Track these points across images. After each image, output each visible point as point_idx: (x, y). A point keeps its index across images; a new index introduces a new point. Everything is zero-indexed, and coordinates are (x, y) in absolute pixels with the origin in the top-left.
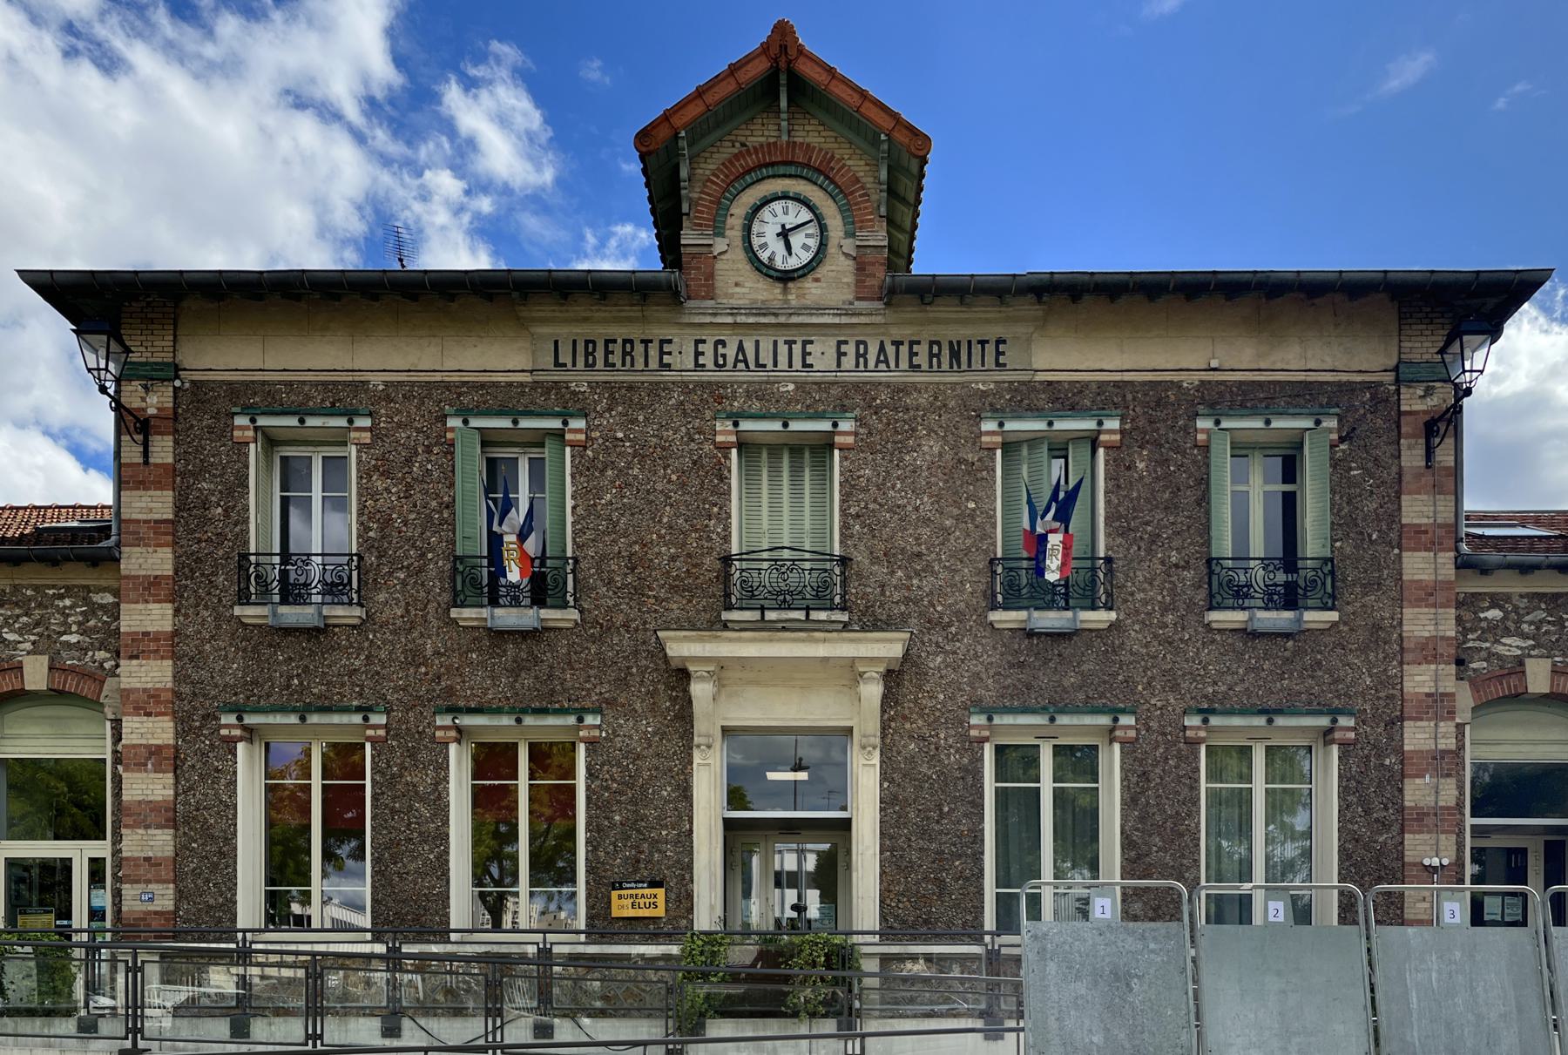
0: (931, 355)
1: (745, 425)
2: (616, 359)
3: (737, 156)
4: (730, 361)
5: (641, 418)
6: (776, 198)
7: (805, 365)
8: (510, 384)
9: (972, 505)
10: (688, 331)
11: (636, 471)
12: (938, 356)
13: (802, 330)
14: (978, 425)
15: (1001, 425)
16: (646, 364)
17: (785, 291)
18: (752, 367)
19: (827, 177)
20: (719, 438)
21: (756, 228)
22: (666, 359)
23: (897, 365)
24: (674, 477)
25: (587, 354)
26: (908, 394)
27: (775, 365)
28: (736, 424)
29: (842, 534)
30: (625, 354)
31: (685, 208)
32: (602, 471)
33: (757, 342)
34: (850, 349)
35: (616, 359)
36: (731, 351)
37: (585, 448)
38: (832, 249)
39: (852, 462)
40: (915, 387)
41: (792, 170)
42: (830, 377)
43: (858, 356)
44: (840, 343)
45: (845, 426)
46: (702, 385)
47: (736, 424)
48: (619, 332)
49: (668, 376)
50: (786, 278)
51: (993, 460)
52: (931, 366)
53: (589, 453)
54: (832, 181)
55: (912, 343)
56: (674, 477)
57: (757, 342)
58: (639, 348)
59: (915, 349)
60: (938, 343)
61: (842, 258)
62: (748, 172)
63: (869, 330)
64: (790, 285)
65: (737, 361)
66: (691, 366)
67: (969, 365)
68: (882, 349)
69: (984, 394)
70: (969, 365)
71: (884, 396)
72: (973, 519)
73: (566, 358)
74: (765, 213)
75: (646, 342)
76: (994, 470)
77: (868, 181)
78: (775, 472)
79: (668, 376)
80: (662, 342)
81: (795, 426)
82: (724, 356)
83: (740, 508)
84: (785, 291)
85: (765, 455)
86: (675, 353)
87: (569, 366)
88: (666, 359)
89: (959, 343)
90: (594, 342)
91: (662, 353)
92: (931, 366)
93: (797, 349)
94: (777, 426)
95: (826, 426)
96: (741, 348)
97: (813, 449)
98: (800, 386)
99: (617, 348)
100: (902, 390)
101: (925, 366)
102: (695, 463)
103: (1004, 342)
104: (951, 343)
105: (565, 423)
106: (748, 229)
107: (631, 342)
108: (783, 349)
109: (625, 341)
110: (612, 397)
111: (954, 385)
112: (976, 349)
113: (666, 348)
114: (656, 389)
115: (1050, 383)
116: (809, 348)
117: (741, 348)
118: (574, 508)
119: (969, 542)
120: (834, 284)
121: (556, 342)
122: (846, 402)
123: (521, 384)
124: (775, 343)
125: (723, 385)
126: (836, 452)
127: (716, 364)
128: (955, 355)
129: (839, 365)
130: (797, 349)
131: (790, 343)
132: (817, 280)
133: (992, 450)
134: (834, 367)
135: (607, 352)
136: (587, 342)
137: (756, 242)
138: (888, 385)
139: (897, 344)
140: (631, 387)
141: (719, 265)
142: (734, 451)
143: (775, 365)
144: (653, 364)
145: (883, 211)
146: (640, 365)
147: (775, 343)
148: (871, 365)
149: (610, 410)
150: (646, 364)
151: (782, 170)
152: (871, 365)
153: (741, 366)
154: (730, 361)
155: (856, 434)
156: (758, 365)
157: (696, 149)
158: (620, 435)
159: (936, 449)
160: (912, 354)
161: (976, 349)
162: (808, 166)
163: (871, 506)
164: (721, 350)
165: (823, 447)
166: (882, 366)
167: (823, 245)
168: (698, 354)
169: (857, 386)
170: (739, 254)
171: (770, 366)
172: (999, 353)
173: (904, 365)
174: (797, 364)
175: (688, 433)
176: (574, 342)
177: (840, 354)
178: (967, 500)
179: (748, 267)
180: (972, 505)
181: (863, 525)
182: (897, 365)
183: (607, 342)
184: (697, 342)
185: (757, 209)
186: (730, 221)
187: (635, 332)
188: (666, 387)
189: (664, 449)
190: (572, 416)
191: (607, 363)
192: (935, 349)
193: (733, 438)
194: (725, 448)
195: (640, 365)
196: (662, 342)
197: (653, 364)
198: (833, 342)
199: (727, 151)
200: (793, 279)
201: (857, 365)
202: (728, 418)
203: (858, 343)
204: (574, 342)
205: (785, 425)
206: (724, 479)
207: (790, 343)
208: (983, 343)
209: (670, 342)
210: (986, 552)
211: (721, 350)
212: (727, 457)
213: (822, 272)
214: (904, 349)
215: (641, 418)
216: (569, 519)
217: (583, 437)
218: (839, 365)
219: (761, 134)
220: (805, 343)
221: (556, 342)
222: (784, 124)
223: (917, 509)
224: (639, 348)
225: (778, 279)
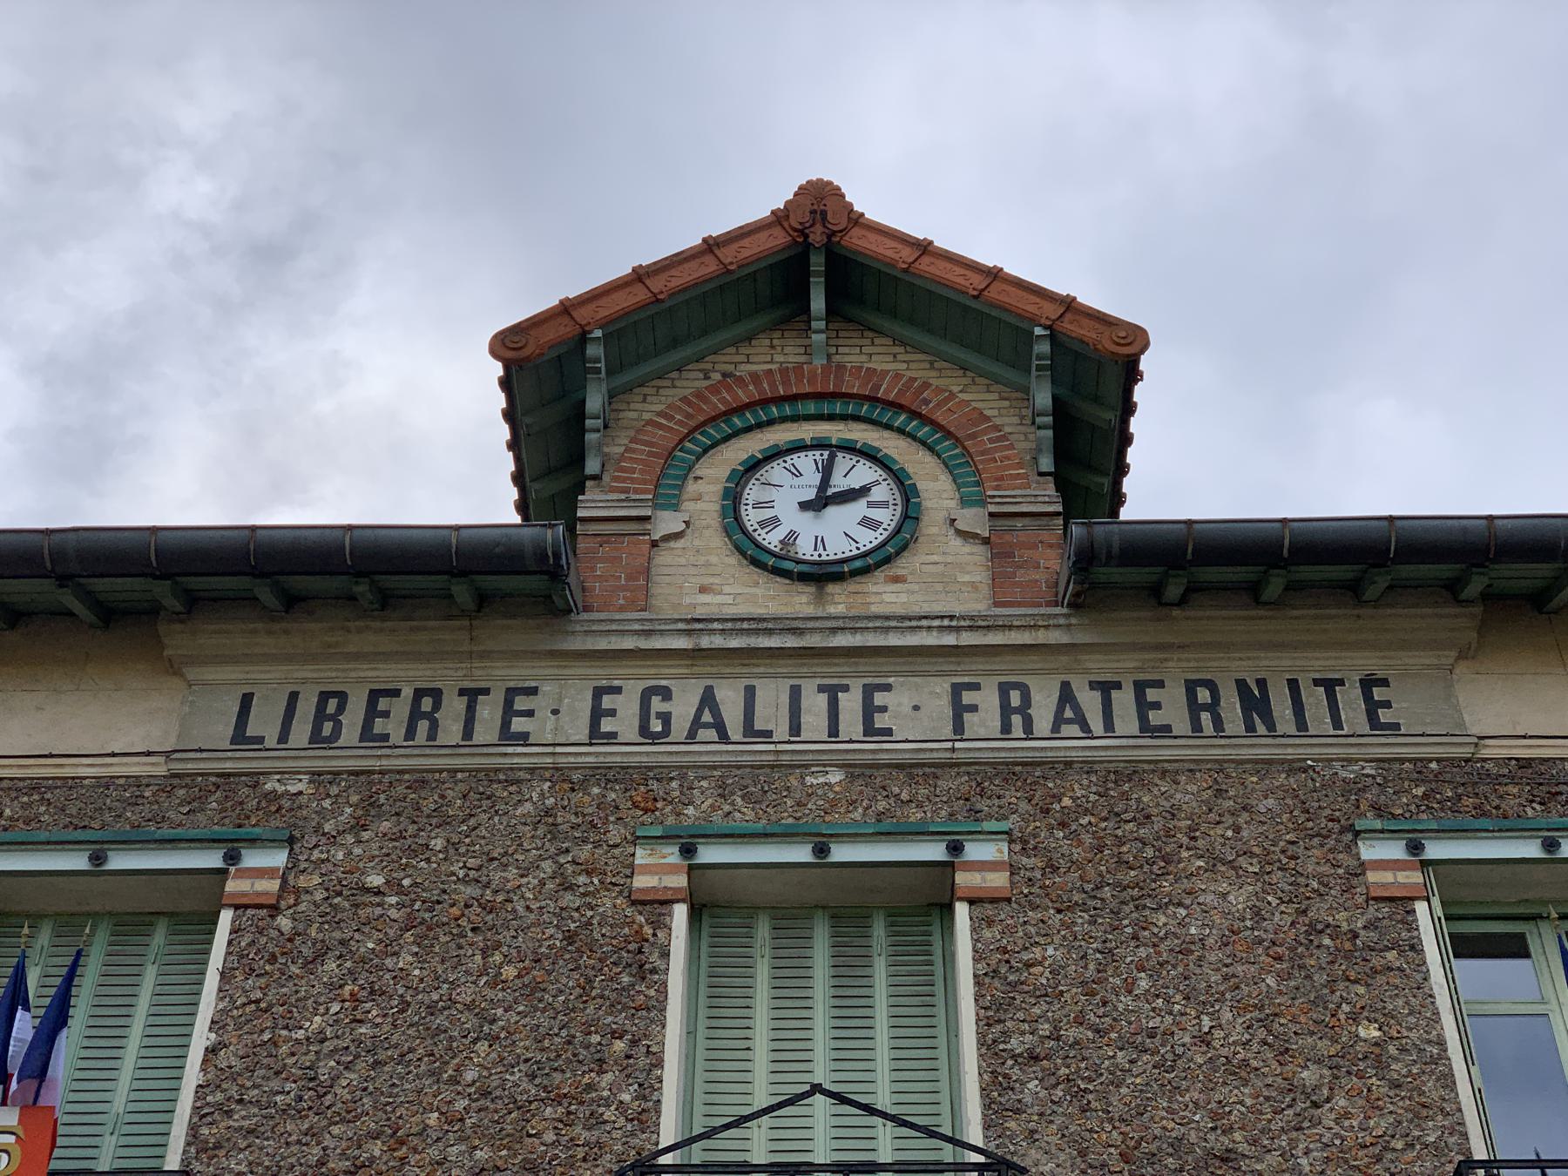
0: (1194, 708)
1: (709, 854)
2: (394, 727)
3: (714, 389)
4: (680, 727)
5: (438, 844)
6: (799, 447)
7: (869, 730)
8: (106, 783)
9: (1370, 1032)
10: (580, 669)
11: (405, 959)
12: (1213, 707)
13: (864, 665)
14: (1350, 849)
15: (1415, 847)
16: (468, 733)
17: (820, 598)
18: (735, 733)
19: (915, 415)
20: (640, 882)
21: (753, 492)
22: (518, 724)
23: (1109, 725)
24: (509, 972)
25: (320, 715)
26: (1147, 786)
27: (795, 729)
28: (688, 851)
29: (988, 1104)
30: (415, 715)
31: (592, 466)
32: (310, 964)
33: (750, 692)
34: (987, 700)
35: (394, 727)
36: (683, 707)
37: (274, 910)
38: (933, 525)
39: (1008, 931)
40: (1165, 770)
41: (838, 408)
42: (938, 752)
43: (1006, 710)
44: (957, 690)
45: (976, 851)
46: (605, 775)
47: (688, 851)
48: (408, 676)
49: (518, 756)
50: (822, 575)
51: (1411, 925)
52: (1197, 727)
53: (284, 922)
54: (926, 420)
55: (1140, 687)
56: (509, 972)
57: (750, 692)
58: (454, 706)
59: (1152, 695)
60: (1211, 685)
61: (957, 542)
62: (740, 410)
63: (1033, 662)
64: (832, 588)
65: (697, 723)
66: (583, 735)
67: (1301, 724)
68: (1066, 695)
69: (1354, 788)
70: (1301, 724)
71: (1080, 789)
72: (1381, 1065)
73: (263, 723)
74: (776, 472)
75: (472, 695)
76: (1416, 948)
77: (1010, 423)
78: (790, 979)
79: (518, 756)
80: (512, 693)
81: (841, 853)
82: (666, 718)
83: (690, 1033)
84: (820, 598)
85: (763, 930)
86: (543, 713)
87: (271, 742)
88: (518, 724)
89: (1262, 683)
90: (342, 697)
91: (509, 711)
92: (1197, 727)
93: (850, 703)
94: (801, 853)
95: (934, 851)
96: (708, 699)
97: (896, 916)
98: (857, 771)
99: (400, 709)
100: (1130, 773)
101: (1181, 725)
102: (570, 937)
103: (1384, 682)
104: (1241, 685)
105: (232, 857)
106: (733, 499)
107: (436, 694)
108: (815, 705)
109: (419, 694)
110: (370, 803)
111: (1264, 766)
112: (1315, 699)
113: (521, 703)
114: (490, 784)
115: (1524, 763)
116: (879, 699)
117: (708, 699)
118: (211, 1051)
119: (1380, 1125)
120: (948, 577)
121: (246, 701)
122: (983, 805)
123: (137, 782)
124: (795, 693)
125: (661, 773)
126: (962, 911)
127: (644, 729)
128: (1255, 703)
129: (959, 727)
130: (850, 703)
131: (832, 693)
132: (897, 579)
133: (1402, 903)
134: (947, 731)
135: (372, 712)
136: (324, 697)
137: (751, 517)
138: (1089, 767)
139: (1106, 688)
140: (421, 780)
141: (663, 558)
142: (680, 912)
143: (795, 729)
144: (487, 730)
145: (1046, 463)
146: (451, 731)
147: (795, 693)
148: (1043, 724)
149: (359, 826)
150: (468, 733)
151: (811, 407)
152: (1043, 724)
153: (712, 734)
154: (680, 727)
155: (1013, 869)
156: (749, 730)
157: (620, 380)
158: (376, 880)
159: (1239, 900)
160: (1143, 706)
161: (1315, 699)
162: (873, 400)
163: (1072, 1033)
164: (657, 704)
165: (925, 902)
166: (1074, 730)
167: (910, 515)
168: (597, 714)
169: (1012, 772)
170: (711, 543)
171: (781, 731)
172: (1372, 708)
173: (1127, 721)
174: (851, 723)
175: (559, 872)
176: (293, 697)
177: (960, 711)
178: (1354, 1018)
179: (734, 560)
180: (1370, 1032)
181: (1050, 1080)
182: (1109, 725)
183: (375, 695)
184: (598, 693)
185: (753, 466)
186: (692, 488)
187: (449, 677)
188: (512, 779)
189: (489, 908)
190: (253, 842)
191: (367, 733)
192: (1204, 695)
193: (681, 881)
194: (658, 904)
195: (451, 731)
196: (512, 693)
197: (487, 730)
198: (943, 686)
199: (691, 382)
200: (838, 577)
201: (1006, 728)
202: (666, 838)
203: (1004, 690)
204: (293, 697)
205: (821, 850)
206: (648, 971)
207: (832, 693)
208: (1330, 685)
209: (533, 691)
210: (1438, 1149)
211: (657, 704)
212: (661, 923)
213: (902, 566)
214: (1124, 700)
215: (438, 844)
216: (192, 1075)
217: (274, 885)
218: (959, 727)
219: (769, 359)
220: (869, 691)
221: (246, 701)
222: (819, 338)
223: (1204, 1040)
224: (454, 706)
225: (803, 578)
